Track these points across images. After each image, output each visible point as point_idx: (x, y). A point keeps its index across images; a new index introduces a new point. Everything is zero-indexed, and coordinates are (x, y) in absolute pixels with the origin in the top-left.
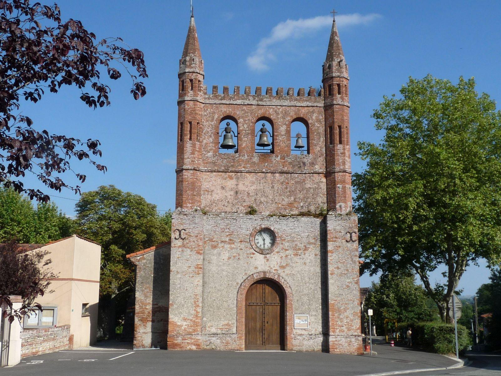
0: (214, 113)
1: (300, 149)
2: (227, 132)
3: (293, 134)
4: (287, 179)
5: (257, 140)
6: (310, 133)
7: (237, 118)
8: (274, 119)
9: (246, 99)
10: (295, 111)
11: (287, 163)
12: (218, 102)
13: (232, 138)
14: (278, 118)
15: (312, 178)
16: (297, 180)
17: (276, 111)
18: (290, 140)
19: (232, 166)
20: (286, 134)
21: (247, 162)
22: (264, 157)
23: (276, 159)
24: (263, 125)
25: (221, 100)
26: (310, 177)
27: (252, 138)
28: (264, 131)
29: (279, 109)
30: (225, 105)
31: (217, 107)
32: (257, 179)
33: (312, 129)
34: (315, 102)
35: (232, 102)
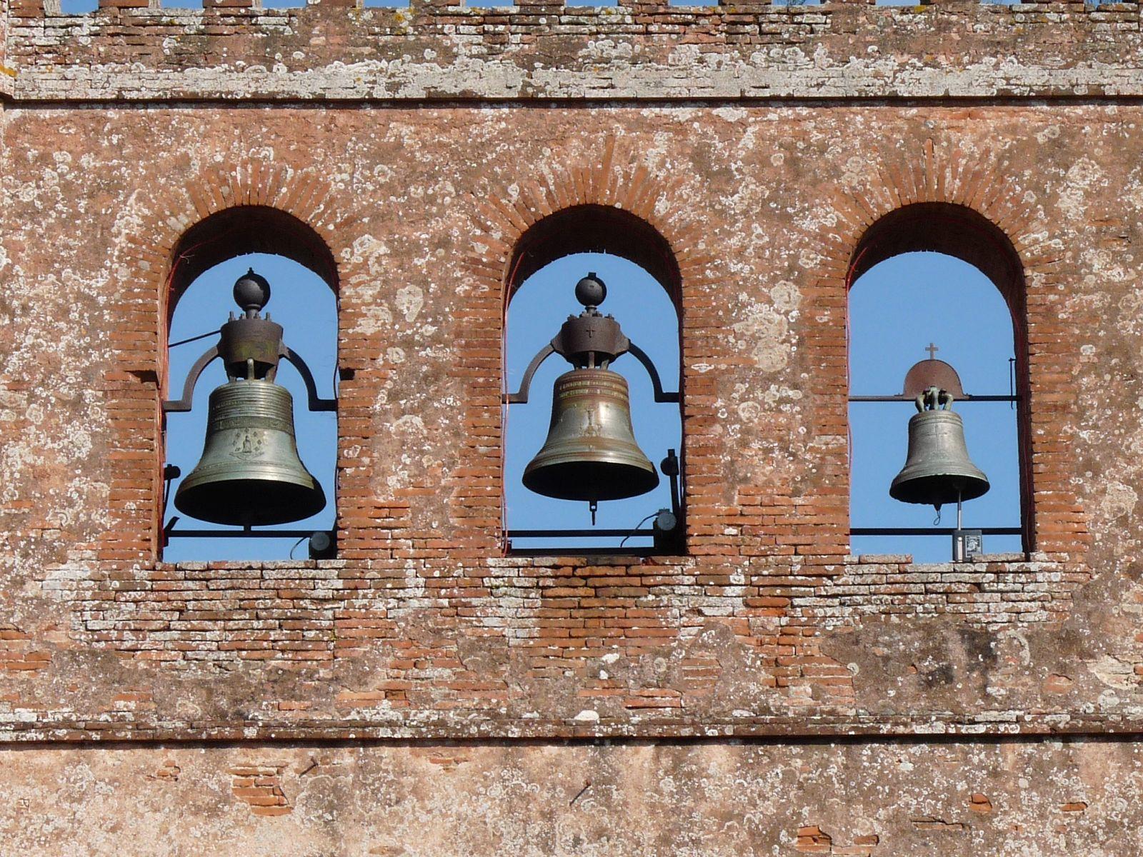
0: (110, 187)
1: (950, 514)
2: (237, 369)
3: (877, 363)
4: (809, 793)
5: (525, 435)
6: (1037, 352)
7: (327, 228)
8: (690, 230)
9: (417, 53)
10: (884, 148)
11: (814, 645)
12: (147, 80)
13: (286, 422)
14: (722, 213)
15: (1060, 778)
16: (906, 800)
17: (700, 157)
18: (842, 427)
19: (282, 684)
20: (799, 362)
21: (424, 641)
22: (592, 584)
23: (700, 610)
24: (590, 294)
25: (179, 61)
26: (1041, 769)
27: (473, 411)
28: (597, 343)
29: (730, 131)
30: (215, 114)
31: (141, 135)
32: (515, 802)
33: (1050, 311)
34: (1080, 55)
35: (279, 80)
